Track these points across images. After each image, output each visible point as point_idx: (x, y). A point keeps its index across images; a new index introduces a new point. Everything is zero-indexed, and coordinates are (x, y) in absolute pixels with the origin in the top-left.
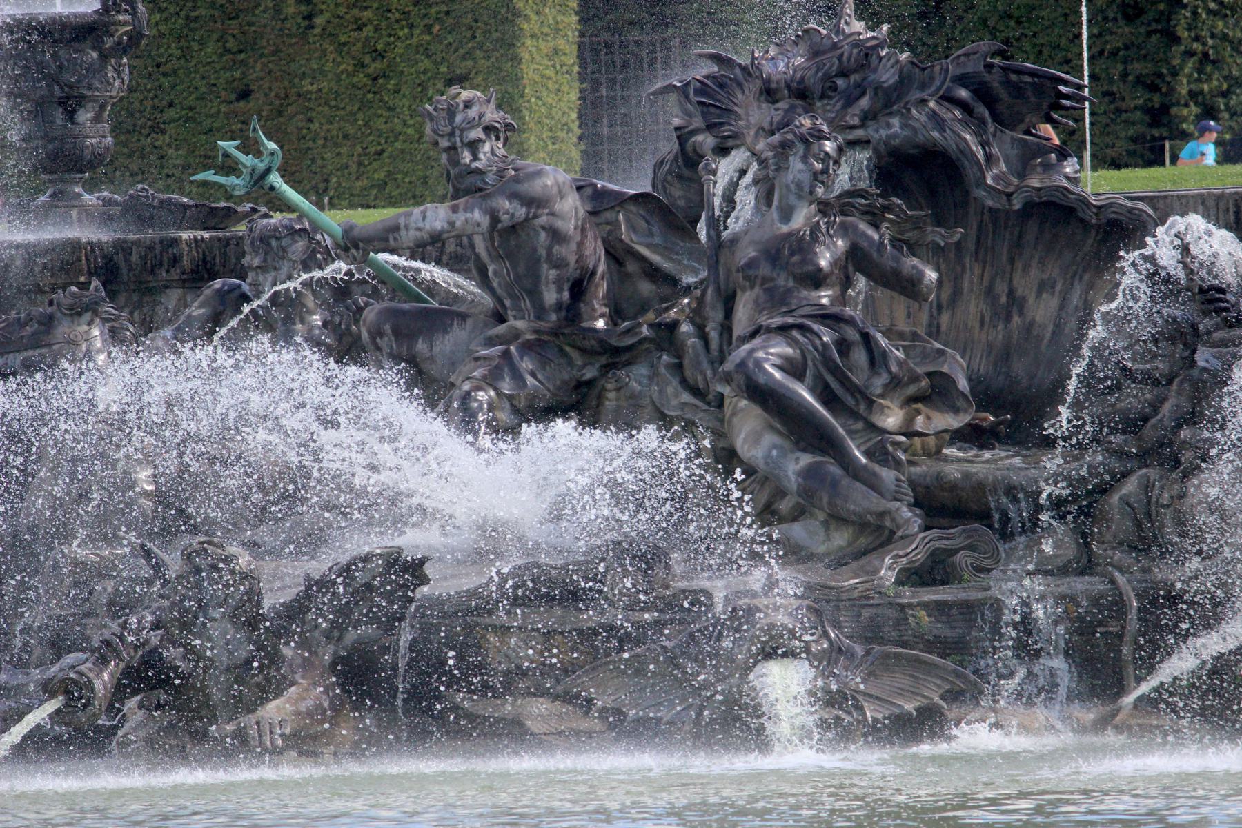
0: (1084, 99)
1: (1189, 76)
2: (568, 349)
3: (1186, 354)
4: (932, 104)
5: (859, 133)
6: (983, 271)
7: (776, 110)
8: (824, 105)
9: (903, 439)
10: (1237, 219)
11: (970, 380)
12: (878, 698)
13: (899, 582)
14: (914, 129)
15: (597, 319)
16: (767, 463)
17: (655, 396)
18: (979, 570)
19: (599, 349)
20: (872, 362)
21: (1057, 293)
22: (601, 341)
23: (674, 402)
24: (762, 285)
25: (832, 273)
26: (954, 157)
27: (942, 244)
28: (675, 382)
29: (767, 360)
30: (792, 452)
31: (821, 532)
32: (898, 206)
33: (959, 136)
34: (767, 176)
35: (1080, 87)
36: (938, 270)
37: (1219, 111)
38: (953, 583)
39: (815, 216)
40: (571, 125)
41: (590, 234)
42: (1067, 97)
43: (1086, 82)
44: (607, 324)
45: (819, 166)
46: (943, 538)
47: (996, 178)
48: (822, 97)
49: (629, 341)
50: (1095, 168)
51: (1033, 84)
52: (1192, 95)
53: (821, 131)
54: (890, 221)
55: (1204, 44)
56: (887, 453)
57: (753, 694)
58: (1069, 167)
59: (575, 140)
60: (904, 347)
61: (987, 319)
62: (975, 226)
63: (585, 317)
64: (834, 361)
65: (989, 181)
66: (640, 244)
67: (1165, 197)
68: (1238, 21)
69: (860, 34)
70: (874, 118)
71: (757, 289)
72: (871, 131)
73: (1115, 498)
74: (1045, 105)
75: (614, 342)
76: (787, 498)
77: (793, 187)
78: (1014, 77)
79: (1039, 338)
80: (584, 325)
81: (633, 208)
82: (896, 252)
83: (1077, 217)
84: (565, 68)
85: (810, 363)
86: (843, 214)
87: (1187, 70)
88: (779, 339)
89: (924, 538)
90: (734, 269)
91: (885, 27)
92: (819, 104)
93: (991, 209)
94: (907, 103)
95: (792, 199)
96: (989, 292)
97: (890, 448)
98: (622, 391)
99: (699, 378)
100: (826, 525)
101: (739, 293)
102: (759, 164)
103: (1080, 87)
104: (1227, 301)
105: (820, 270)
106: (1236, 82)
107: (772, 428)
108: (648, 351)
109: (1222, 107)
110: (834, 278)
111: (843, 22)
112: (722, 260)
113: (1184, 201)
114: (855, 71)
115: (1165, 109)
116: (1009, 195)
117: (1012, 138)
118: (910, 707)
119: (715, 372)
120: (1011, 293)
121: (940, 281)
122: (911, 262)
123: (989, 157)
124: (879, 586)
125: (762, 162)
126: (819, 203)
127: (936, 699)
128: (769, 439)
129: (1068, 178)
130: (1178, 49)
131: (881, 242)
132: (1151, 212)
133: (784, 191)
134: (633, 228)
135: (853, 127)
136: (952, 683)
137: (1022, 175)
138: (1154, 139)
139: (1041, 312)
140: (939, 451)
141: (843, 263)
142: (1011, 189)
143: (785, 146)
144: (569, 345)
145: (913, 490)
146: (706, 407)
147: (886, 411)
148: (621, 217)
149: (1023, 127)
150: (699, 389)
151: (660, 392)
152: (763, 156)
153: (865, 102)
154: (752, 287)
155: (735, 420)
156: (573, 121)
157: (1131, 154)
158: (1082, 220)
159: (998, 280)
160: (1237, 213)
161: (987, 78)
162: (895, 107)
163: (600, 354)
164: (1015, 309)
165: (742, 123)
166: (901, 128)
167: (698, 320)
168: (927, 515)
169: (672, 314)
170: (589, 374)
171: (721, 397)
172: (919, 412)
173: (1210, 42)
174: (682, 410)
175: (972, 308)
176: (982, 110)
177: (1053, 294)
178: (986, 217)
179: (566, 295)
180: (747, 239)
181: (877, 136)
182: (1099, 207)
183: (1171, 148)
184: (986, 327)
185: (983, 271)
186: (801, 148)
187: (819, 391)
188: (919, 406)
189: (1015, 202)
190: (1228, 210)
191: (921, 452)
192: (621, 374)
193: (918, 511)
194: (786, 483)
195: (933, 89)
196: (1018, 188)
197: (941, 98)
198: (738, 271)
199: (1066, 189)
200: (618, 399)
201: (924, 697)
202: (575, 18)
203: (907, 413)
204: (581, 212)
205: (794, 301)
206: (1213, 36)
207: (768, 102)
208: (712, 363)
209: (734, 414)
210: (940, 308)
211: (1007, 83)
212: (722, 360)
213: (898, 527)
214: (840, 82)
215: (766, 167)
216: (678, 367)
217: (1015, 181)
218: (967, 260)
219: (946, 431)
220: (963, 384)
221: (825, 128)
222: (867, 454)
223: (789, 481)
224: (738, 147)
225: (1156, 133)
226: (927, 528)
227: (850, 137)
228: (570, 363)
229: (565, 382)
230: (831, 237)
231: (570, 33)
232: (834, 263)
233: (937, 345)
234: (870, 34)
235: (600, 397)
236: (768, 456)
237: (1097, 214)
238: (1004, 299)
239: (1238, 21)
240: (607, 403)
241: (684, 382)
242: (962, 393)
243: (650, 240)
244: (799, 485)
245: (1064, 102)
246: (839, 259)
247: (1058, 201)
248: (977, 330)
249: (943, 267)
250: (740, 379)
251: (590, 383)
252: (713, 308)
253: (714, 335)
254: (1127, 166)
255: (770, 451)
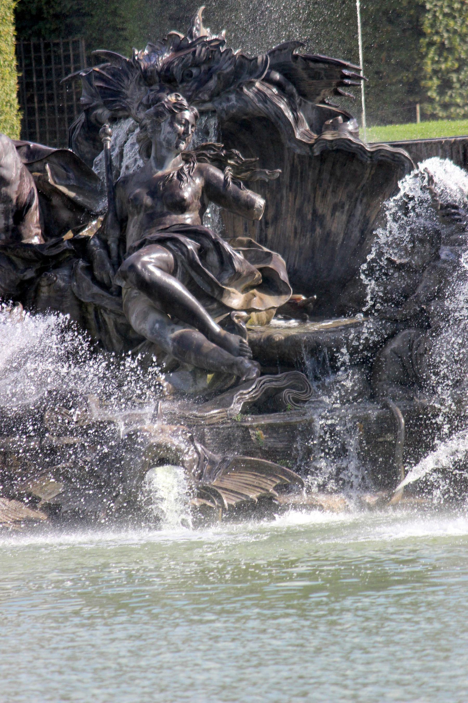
0: (360, 78)
1: (432, 59)
2: (14, 258)
3: (434, 251)
4: (257, 84)
5: (209, 106)
6: (295, 199)
7: (151, 90)
8: (183, 87)
9: (244, 314)
10: (465, 160)
11: (289, 273)
12: (232, 491)
13: (244, 412)
14: (246, 102)
15: (32, 237)
16: (152, 333)
17: (75, 289)
18: (297, 401)
19: (36, 258)
20: (222, 262)
21: (345, 212)
22: (35, 253)
23: (88, 293)
24: (145, 211)
25: (193, 202)
26: (273, 120)
27: (267, 180)
28: (88, 279)
29: (150, 263)
30: (169, 325)
31: (191, 378)
32: (236, 155)
33: (276, 106)
34: (147, 136)
35: (359, 71)
36: (264, 197)
37: (453, 83)
38: (280, 411)
39: (180, 163)
40: (12, 102)
41: (26, 179)
42: (348, 77)
43: (361, 67)
44: (40, 240)
45: (181, 129)
46: (272, 381)
47: (303, 134)
48: (182, 81)
49: (55, 252)
50: (368, 126)
51: (325, 70)
52: (435, 72)
53: (181, 105)
54: (232, 166)
55: (442, 37)
56: (234, 323)
57: (190, 491)
58: (350, 126)
59: (15, 112)
60: (243, 251)
61: (299, 231)
62: (289, 168)
63: (25, 236)
64: (196, 262)
65: (298, 137)
66: (61, 184)
67: (416, 144)
68: (463, 22)
69: (206, 37)
70: (218, 95)
71: (142, 214)
72: (216, 104)
73: (388, 351)
74: (334, 83)
75: (45, 253)
76: (167, 356)
77: (164, 143)
78: (312, 65)
79: (335, 243)
80: (24, 241)
81: (55, 160)
82: (236, 187)
83: (358, 160)
84: (6, 63)
85: (179, 264)
86: (199, 161)
87: (430, 55)
88: (159, 247)
89: (261, 381)
90: (125, 201)
91: (224, 32)
92: (180, 86)
93: (299, 156)
94: (241, 84)
95: (164, 152)
96: (300, 213)
97: (236, 321)
98: (52, 286)
99: (105, 276)
100: (194, 373)
101: (130, 218)
102: (141, 129)
103: (359, 71)
104: (459, 214)
105: (183, 200)
106: (462, 63)
107: (154, 309)
108: (69, 259)
109: (455, 80)
110: (194, 205)
111: (194, 28)
112: (118, 195)
113: (429, 147)
114: (204, 62)
115: (416, 82)
116: (311, 146)
117: (313, 108)
118: (254, 496)
119: (115, 271)
120: (315, 212)
121: (266, 206)
122: (248, 193)
123: (297, 119)
124: (231, 415)
125: (143, 128)
126: (183, 154)
127: (271, 490)
128: (154, 316)
129: (351, 133)
130: (424, 41)
131: (226, 180)
132: (407, 154)
133: (159, 146)
134: (55, 174)
135: (204, 102)
136: (281, 479)
137: (319, 132)
138: (410, 103)
139: (335, 225)
140: (268, 322)
141: (200, 195)
142: (312, 142)
143: (159, 114)
144: (15, 255)
145: (253, 349)
146: (110, 296)
147: (232, 294)
148: (47, 167)
149: (319, 98)
150: (104, 284)
151: (78, 286)
152: (144, 123)
153: (212, 84)
154: (139, 213)
155: (130, 304)
156: (13, 100)
157: (394, 114)
158: (361, 162)
159: (306, 204)
160: (465, 154)
161: (294, 65)
162: (232, 87)
163: (36, 261)
164: (317, 223)
165: (129, 100)
166: (236, 101)
167: (103, 237)
168: (262, 365)
169: (84, 233)
170: (29, 274)
171: (120, 289)
172: (254, 295)
173: (446, 35)
174: (93, 298)
175: (289, 223)
176: (291, 88)
177: (343, 212)
178: (296, 161)
179: (11, 221)
180: (135, 179)
181: (220, 107)
182: (372, 153)
183: (421, 109)
184: (298, 236)
185: (295, 199)
186: (168, 116)
187: (186, 283)
188: (255, 291)
189: (315, 150)
190: (458, 152)
191: (257, 322)
192: (51, 275)
193: (256, 363)
194: (166, 346)
195: (258, 73)
196: (317, 140)
197: (263, 80)
198: (129, 202)
199: (350, 140)
200: (49, 292)
201: (262, 488)
202: (12, 28)
203: (246, 297)
204: (20, 165)
205: (168, 222)
206: (448, 31)
207: (146, 85)
208: (113, 265)
209: (128, 301)
210: (267, 223)
211: (307, 68)
212: (119, 263)
213: (243, 375)
214: (195, 71)
215: (146, 130)
216: (89, 269)
217: (315, 136)
218: (284, 192)
219: (274, 308)
220: (283, 275)
221: (185, 103)
222: (221, 324)
223: (168, 344)
224: (127, 117)
225: (411, 99)
226: (262, 374)
227: (202, 108)
228: (15, 267)
229: (12, 281)
230: (191, 177)
231: (9, 39)
232: (194, 194)
233: (266, 249)
234: (214, 37)
235: (37, 291)
236: (152, 329)
237: (371, 157)
238: (310, 217)
239: (463, 22)
240: (42, 294)
241: (94, 279)
242: (284, 282)
243: (68, 182)
244: (174, 347)
245: (346, 81)
246: (197, 192)
247: (345, 149)
248: (292, 239)
249: (268, 196)
250: (132, 276)
251: (31, 281)
252: (113, 228)
253: (113, 246)
254: (391, 123)
255: (154, 325)
